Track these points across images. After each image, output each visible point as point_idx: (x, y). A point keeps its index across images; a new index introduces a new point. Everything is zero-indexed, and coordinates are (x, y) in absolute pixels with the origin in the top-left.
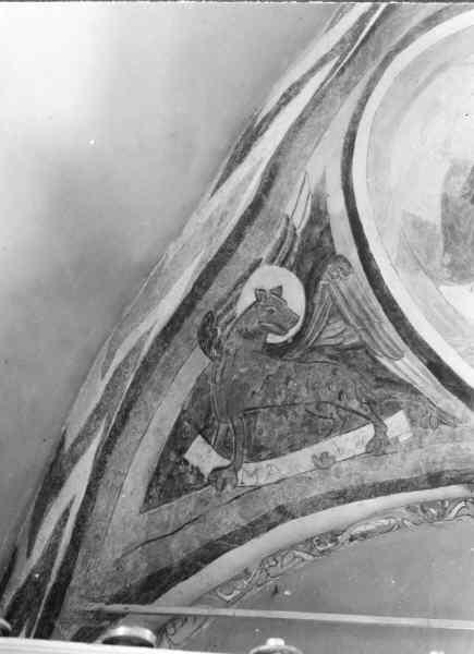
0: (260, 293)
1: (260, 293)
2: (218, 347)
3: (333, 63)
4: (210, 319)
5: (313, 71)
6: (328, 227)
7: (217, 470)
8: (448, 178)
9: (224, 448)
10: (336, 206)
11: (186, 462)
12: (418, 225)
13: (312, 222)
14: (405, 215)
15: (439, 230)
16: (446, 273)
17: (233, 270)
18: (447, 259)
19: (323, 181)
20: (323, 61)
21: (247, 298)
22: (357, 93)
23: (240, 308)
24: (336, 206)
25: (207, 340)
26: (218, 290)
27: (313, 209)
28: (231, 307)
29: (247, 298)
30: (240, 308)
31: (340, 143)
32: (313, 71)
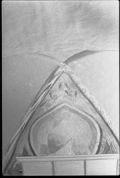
0: (17, 165)
1: (17, 165)
3: (19, 135)
4: (9, 171)
5: (16, 137)
6: (27, 152)
8: (48, 136)
10: (28, 148)
12: (44, 146)
13: (24, 152)
17: (12, 163)
19: (25, 145)
20: (17, 135)
21: (15, 166)
22: (28, 132)
23: (14, 168)
24: (28, 148)
26: (10, 167)
28: (13, 168)
29: (15, 166)
30: (14, 168)
31: (27, 139)
32: (16, 137)
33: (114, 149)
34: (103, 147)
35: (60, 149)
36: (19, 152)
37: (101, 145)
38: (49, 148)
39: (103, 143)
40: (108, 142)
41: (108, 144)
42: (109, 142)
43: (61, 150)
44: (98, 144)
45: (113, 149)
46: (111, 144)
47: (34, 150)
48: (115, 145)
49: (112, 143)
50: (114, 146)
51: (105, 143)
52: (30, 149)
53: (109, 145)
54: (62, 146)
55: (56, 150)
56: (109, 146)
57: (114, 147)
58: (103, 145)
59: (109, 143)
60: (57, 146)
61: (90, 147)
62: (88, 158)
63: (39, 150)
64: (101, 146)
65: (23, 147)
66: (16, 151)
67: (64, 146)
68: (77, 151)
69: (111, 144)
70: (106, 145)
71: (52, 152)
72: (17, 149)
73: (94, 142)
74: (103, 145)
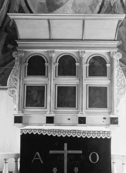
2: (8, 31)
4: (5, 28)
7: (13, 48)
9: (13, 45)
10: (24, 5)
11: (8, 48)
12: (41, 3)
14: (38, 2)
15: (45, 4)
16: (47, 11)
18: (47, 9)
19: (20, 2)
24: (24, 5)
25: (6, 31)
27: (19, 8)
28: (9, 25)
33: (116, 10)
34: (105, 7)
35: (59, 8)
36: (15, 9)
37: (103, 5)
38: (47, 7)
39: (106, 3)
40: (111, 2)
41: (110, 4)
42: (112, 2)
43: (60, 8)
44: (100, 4)
45: (115, 10)
46: (114, 5)
47: (31, 8)
48: (118, 6)
49: (116, 3)
50: (117, 7)
51: (109, 2)
52: (26, 7)
53: (112, 5)
54: (62, 4)
55: (55, 9)
56: (111, 7)
57: (117, 8)
58: (105, 5)
59: (112, 3)
60: (56, 4)
61: (91, 7)
62: (87, 17)
63: (36, 9)
64: (103, 7)
65: (18, 3)
66: (11, 8)
67: (63, 5)
68: (77, 11)
69: (114, 5)
70: (109, 5)
71: (50, 11)
72: (12, 6)
73: (97, 2)
74: (105, 5)
